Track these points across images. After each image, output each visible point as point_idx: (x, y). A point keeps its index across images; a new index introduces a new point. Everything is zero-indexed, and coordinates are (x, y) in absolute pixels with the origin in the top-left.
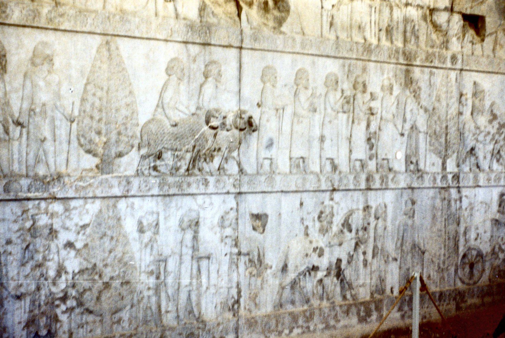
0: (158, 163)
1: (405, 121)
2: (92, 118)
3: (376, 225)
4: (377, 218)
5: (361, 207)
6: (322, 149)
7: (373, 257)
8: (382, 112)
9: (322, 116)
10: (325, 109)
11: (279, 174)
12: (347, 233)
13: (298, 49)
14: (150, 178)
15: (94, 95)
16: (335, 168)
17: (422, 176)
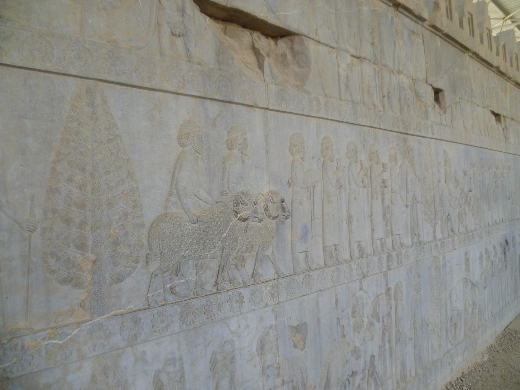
0: (176, 281)
1: (407, 192)
2: (68, 221)
3: (396, 306)
4: (396, 300)
5: (384, 291)
6: (350, 231)
7: (396, 344)
8: (391, 184)
9: (348, 193)
10: (350, 184)
11: (316, 269)
12: (376, 324)
13: (322, 114)
14: (168, 308)
15: (70, 180)
16: (361, 250)
17: (423, 247)
